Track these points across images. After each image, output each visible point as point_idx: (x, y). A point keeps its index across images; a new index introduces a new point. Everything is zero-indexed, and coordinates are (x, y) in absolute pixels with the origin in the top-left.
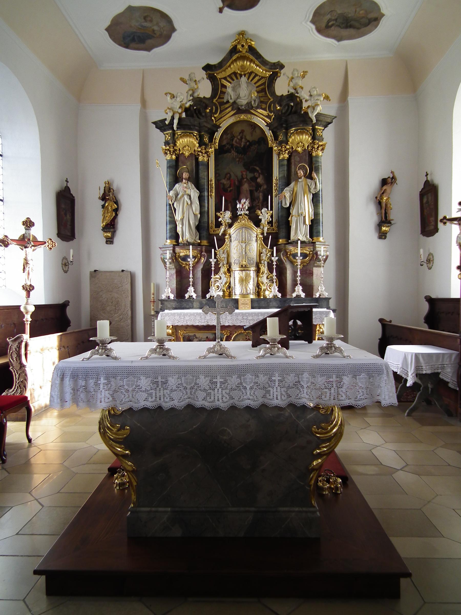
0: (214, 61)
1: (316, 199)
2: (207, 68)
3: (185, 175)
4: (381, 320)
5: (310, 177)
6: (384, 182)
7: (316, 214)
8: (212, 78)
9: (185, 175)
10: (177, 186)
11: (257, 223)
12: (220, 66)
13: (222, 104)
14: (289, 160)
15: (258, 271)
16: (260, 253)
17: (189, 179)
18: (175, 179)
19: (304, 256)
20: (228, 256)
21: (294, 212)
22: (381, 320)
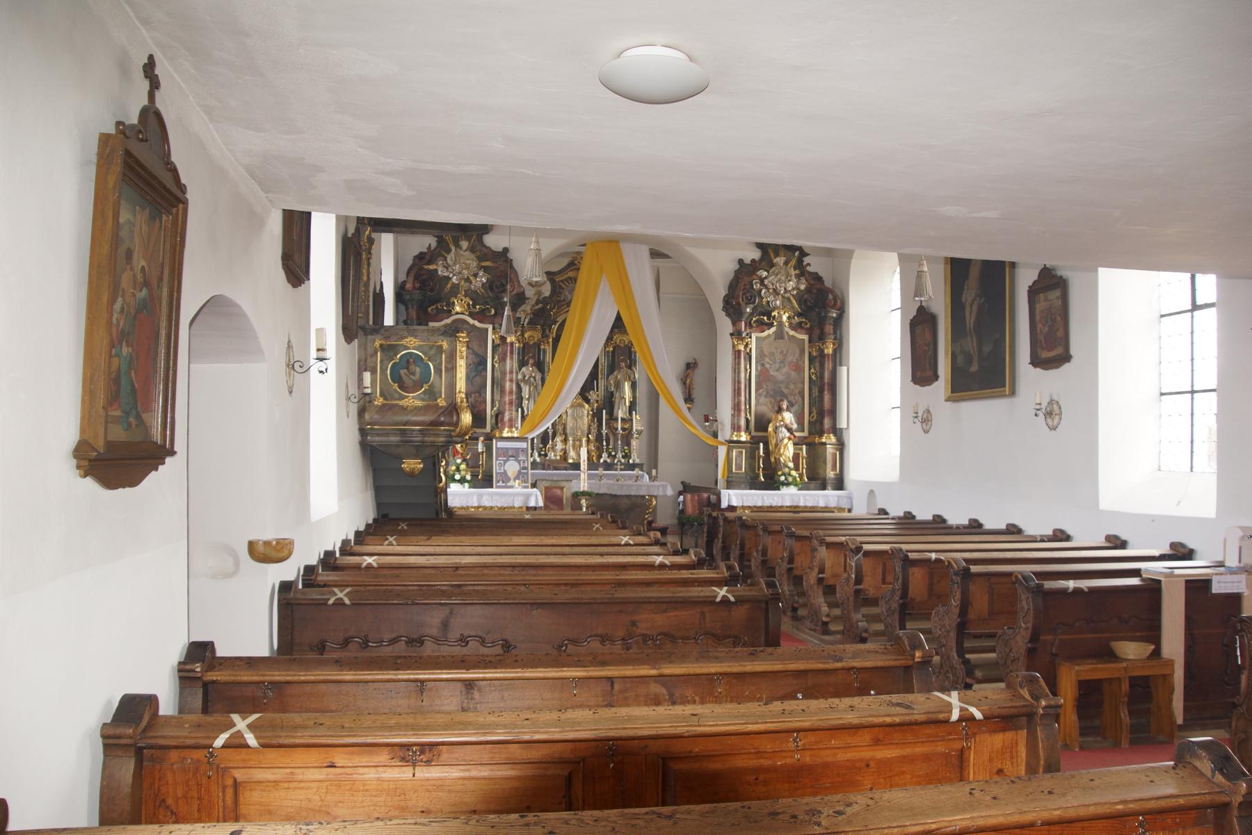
0: (555, 269)
1: (634, 386)
2: (548, 273)
3: (531, 361)
4: (683, 483)
5: (630, 367)
6: (688, 366)
7: (634, 397)
8: (552, 281)
9: (531, 361)
10: (524, 369)
11: (588, 401)
12: (560, 272)
13: (559, 302)
14: (613, 352)
15: (588, 441)
16: (589, 426)
17: (532, 365)
18: (522, 364)
19: (623, 429)
20: (565, 429)
21: (617, 395)
22: (683, 483)
